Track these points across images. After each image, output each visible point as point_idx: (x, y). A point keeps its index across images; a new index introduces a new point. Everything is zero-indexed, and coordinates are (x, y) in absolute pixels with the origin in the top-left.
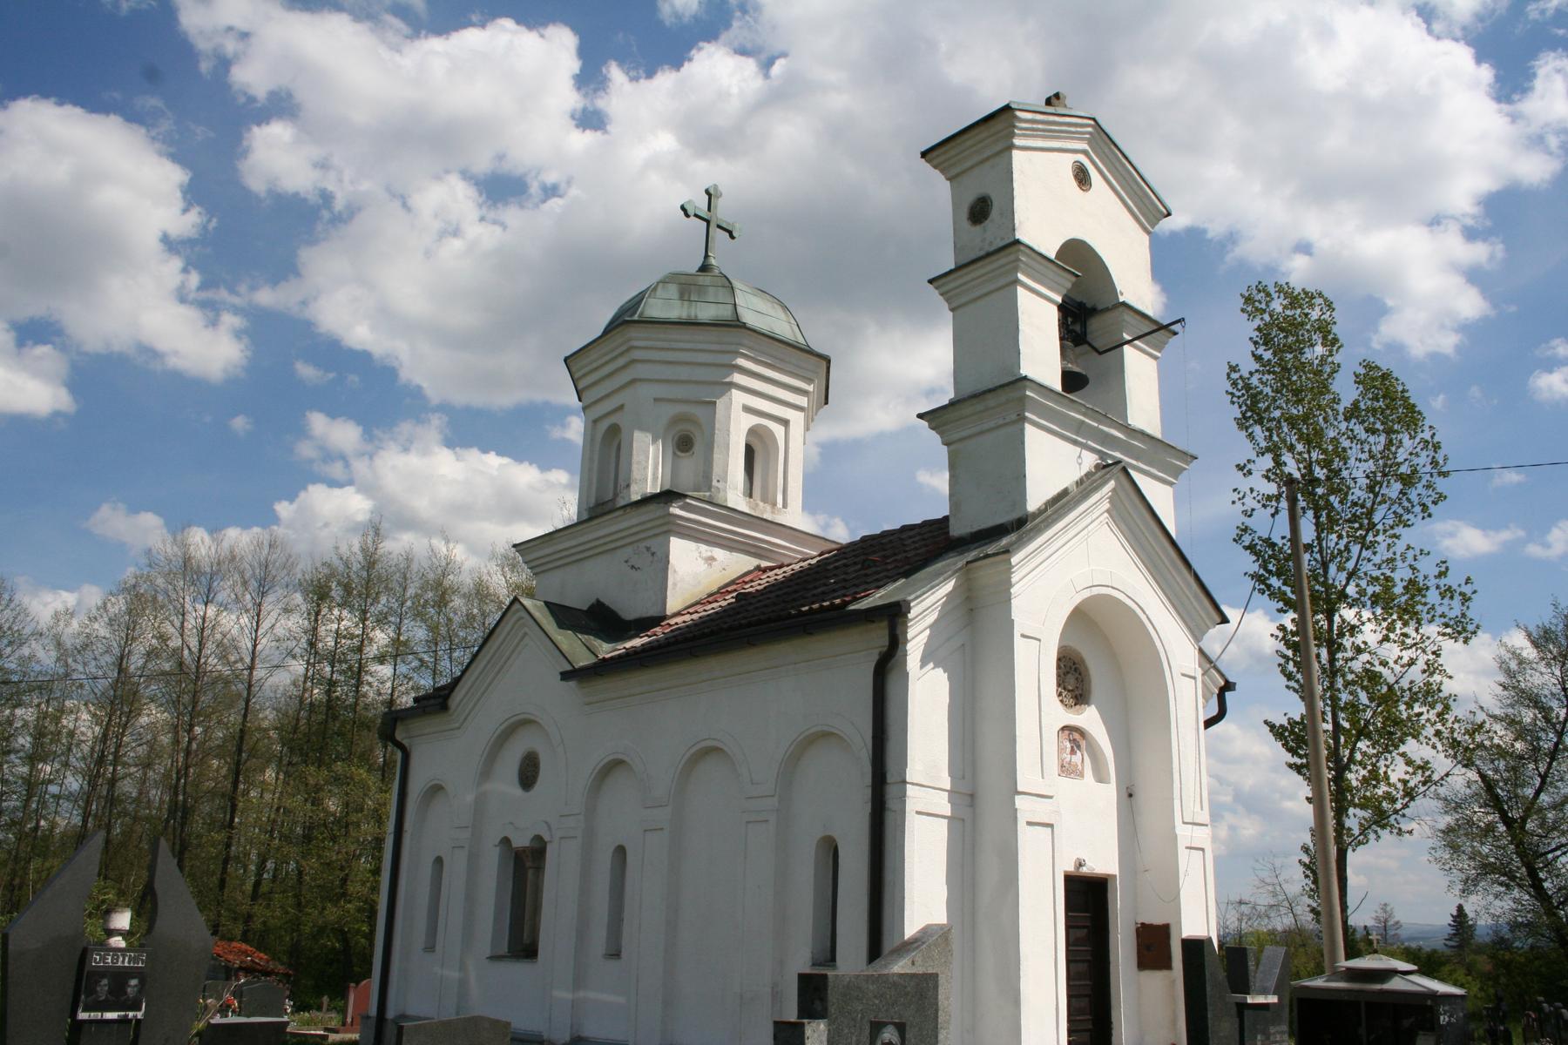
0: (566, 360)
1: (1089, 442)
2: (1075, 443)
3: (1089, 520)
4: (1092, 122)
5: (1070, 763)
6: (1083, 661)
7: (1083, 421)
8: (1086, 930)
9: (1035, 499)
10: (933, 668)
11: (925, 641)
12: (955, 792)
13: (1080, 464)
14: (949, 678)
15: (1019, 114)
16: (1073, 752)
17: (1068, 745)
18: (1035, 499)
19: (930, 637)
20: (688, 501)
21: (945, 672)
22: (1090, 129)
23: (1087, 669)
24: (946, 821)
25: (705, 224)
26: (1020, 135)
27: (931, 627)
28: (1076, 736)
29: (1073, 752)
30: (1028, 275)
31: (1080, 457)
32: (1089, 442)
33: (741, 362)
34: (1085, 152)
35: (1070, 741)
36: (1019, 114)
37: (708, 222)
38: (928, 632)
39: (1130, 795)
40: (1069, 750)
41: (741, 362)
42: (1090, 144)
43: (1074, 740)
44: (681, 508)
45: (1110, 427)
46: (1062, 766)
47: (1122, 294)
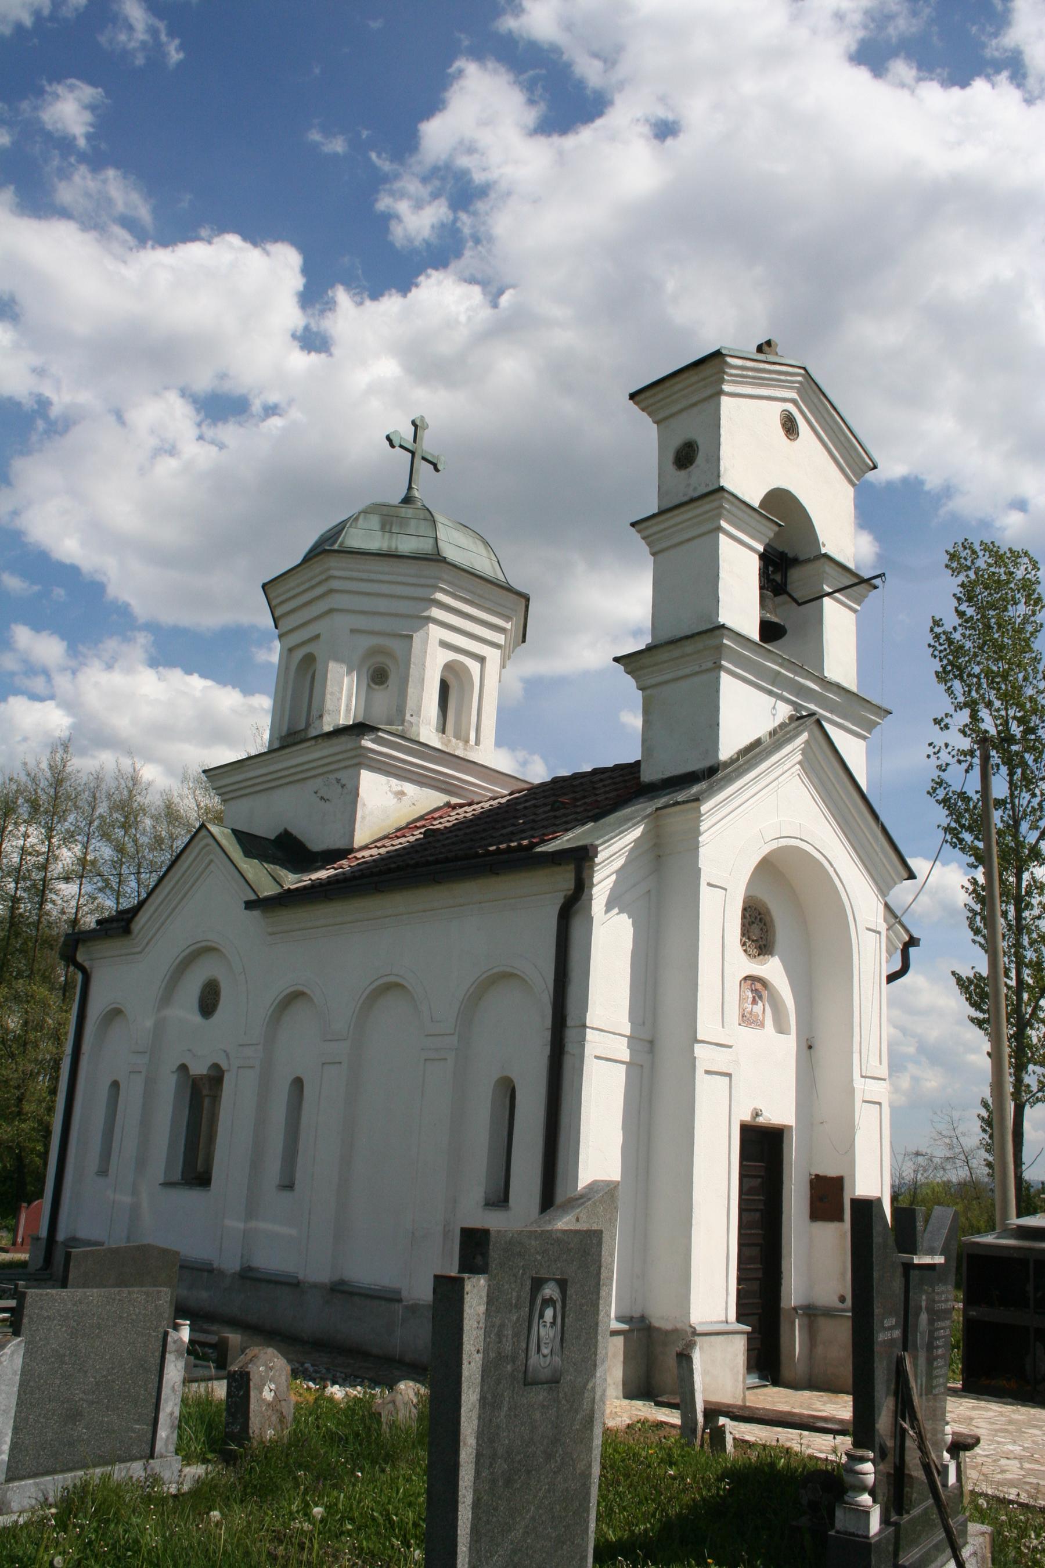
0: (264, 586)
1: (785, 694)
2: (770, 693)
3: (780, 771)
4: (802, 371)
5: (751, 1013)
6: (768, 912)
7: (780, 672)
8: (759, 1180)
9: (727, 748)
10: (617, 914)
11: (611, 885)
12: (636, 1038)
13: (774, 715)
14: (634, 925)
15: (729, 360)
16: (754, 1002)
17: (750, 995)
18: (727, 748)
19: (616, 882)
20: (380, 734)
21: (629, 918)
22: (800, 378)
23: (772, 921)
24: (624, 1067)
25: (410, 455)
26: (729, 382)
27: (617, 872)
28: (759, 986)
29: (754, 1002)
31: (774, 708)
32: (785, 694)
33: (440, 596)
34: (793, 401)
35: (752, 990)
36: (729, 360)
37: (413, 453)
38: (614, 877)
39: (810, 1047)
40: (750, 1000)
41: (440, 596)
42: (799, 393)
43: (756, 990)
44: (373, 741)
46: (743, 1016)
47: (824, 545)
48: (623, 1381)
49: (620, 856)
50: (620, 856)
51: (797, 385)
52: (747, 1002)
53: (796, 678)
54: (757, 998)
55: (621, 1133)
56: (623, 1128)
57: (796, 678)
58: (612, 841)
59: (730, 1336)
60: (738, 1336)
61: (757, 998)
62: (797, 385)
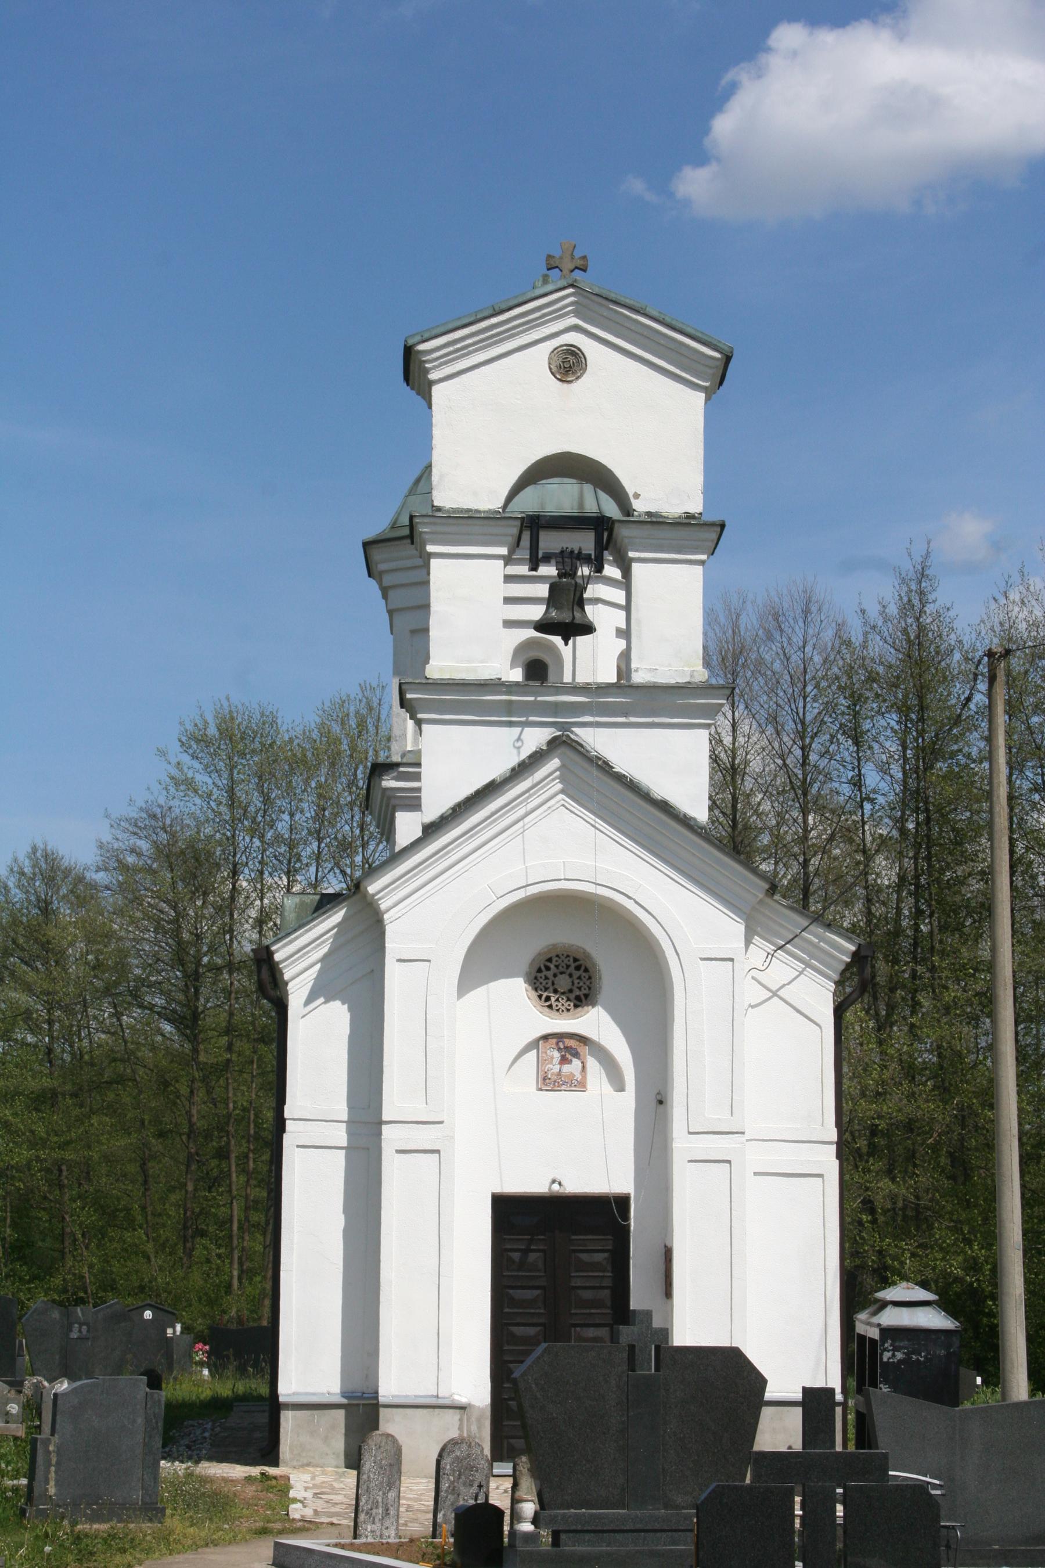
1: (531, 718)
2: (511, 724)
3: (521, 812)
4: (571, 290)
5: (559, 1073)
6: (588, 956)
7: (510, 702)
8: (606, 1255)
10: (325, 1003)
11: (314, 976)
12: (353, 1122)
13: (519, 748)
14: (350, 1009)
15: (421, 347)
16: (564, 1060)
17: (557, 1055)
19: (321, 972)
20: (402, 769)
21: (343, 1004)
22: (572, 299)
23: (594, 965)
24: (343, 1152)
26: (435, 367)
27: (323, 959)
29: (564, 1060)
30: (435, 543)
31: (519, 739)
34: (576, 328)
35: (559, 1049)
36: (421, 347)
38: (319, 966)
39: (661, 1102)
42: (577, 314)
44: (397, 779)
45: (557, 694)
46: (544, 1079)
47: (637, 496)
48: (345, 1451)
49: (323, 942)
50: (323, 942)
51: (570, 308)
52: (551, 1063)
53: (539, 699)
54: (568, 1056)
55: (342, 1217)
56: (347, 1210)
57: (539, 699)
58: (293, 936)
59: (437, 1411)
60: (451, 1411)
61: (568, 1056)
62: (570, 308)
